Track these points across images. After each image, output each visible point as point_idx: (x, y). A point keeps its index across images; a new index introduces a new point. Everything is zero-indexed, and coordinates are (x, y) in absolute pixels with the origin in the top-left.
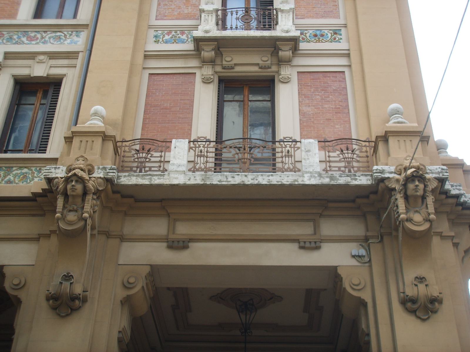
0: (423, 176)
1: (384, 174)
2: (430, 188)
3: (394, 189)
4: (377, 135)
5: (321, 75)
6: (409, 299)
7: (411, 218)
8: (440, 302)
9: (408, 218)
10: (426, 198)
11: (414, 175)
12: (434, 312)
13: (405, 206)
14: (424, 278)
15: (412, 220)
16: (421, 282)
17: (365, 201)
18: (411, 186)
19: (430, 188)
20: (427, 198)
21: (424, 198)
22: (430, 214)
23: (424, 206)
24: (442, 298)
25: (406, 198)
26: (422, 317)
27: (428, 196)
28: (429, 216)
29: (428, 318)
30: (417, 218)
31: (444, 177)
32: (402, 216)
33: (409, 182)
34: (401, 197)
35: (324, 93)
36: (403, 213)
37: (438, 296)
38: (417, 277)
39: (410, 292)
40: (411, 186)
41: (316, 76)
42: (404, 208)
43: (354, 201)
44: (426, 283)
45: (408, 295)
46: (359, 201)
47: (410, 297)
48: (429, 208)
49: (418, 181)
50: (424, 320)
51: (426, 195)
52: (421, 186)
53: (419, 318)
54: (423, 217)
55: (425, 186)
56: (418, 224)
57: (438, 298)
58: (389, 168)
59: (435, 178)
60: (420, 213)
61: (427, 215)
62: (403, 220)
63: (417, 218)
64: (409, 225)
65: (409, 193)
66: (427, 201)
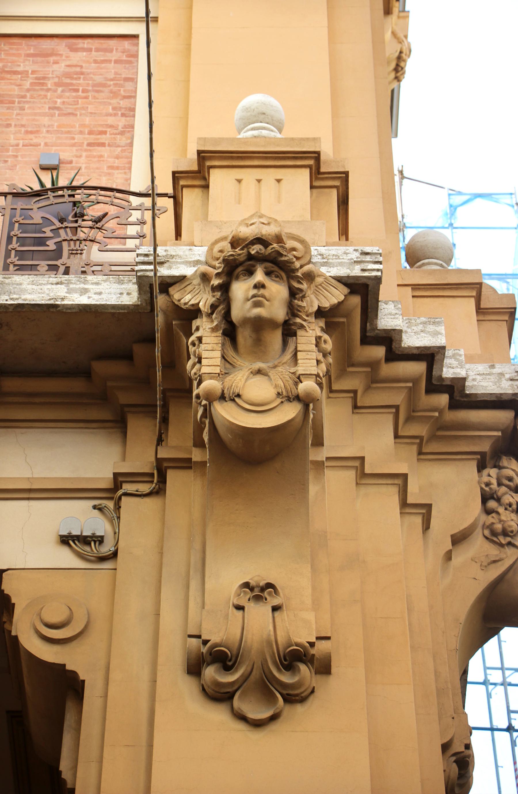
0: (283, 259)
1: (170, 268)
2: (312, 302)
3: (195, 312)
4: (175, 170)
5: (61, 46)
6: (210, 652)
7: (237, 391)
8: (324, 668)
9: (225, 391)
10: (295, 334)
11: (253, 252)
12: (295, 697)
13: (223, 357)
14: (269, 585)
15: (239, 396)
16: (258, 598)
17: (118, 368)
18: (240, 289)
19: (312, 302)
20: (300, 333)
21: (289, 331)
22: (302, 378)
23: (288, 355)
24: (330, 653)
25: (230, 332)
26: (252, 715)
27: (302, 327)
28: (296, 384)
29: (274, 718)
30: (259, 390)
31: (366, 274)
32: (207, 384)
33: (237, 278)
34: (214, 330)
35: (63, 91)
36: (211, 376)
37: (312, 644)
38: (246, 585)
39: (220, 631)
40: (240, 289)
41: (46, 45)
42: (218, 361)
43: (87, 374)
44: (276, 602)
45: (209, 641)
46: (100, 368)
47: (216, 645)
48: (299, 361)
49: (268, 273)
50: (257, 724)
51: (295, 324)
52: (277, 290)
53: (242, 718)
54: (276, 386)
55: (293, 293)
56: (259, 408)
57: (313, 651)
58: (190, 250)
59: (339, 279)
60: (269, 376)
61: (291, 382)
62: (210, 397)
63: (259, 390)
64: (226, 413)
65: (237, 312)
66: (299, 341)
